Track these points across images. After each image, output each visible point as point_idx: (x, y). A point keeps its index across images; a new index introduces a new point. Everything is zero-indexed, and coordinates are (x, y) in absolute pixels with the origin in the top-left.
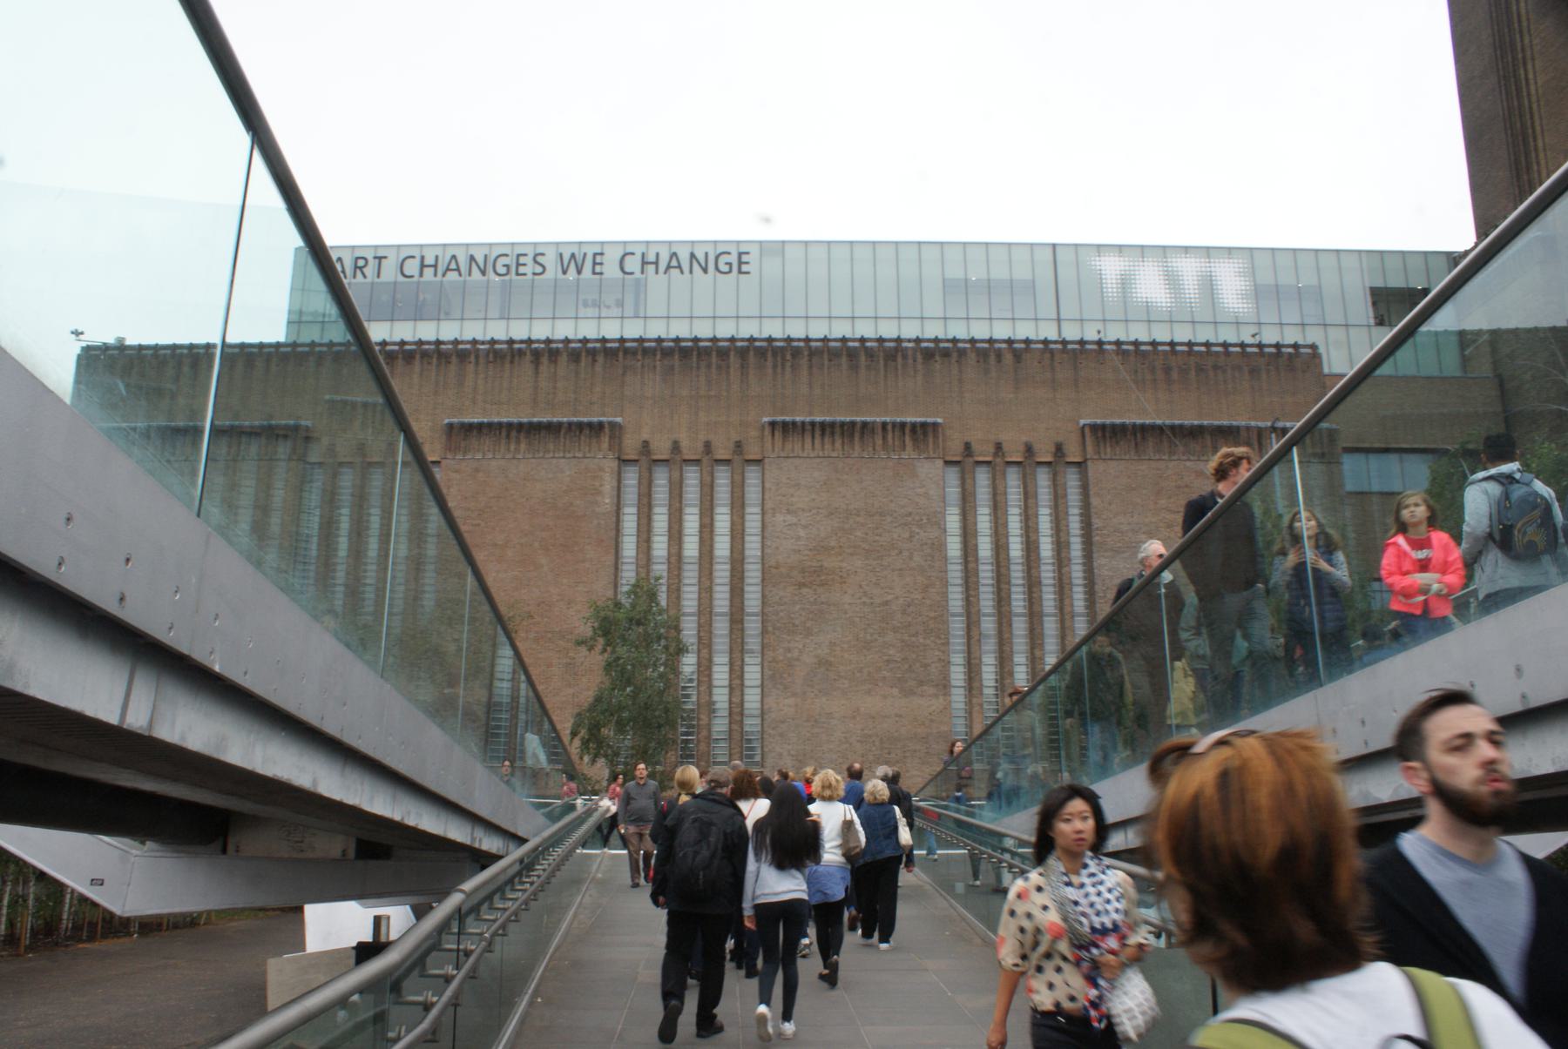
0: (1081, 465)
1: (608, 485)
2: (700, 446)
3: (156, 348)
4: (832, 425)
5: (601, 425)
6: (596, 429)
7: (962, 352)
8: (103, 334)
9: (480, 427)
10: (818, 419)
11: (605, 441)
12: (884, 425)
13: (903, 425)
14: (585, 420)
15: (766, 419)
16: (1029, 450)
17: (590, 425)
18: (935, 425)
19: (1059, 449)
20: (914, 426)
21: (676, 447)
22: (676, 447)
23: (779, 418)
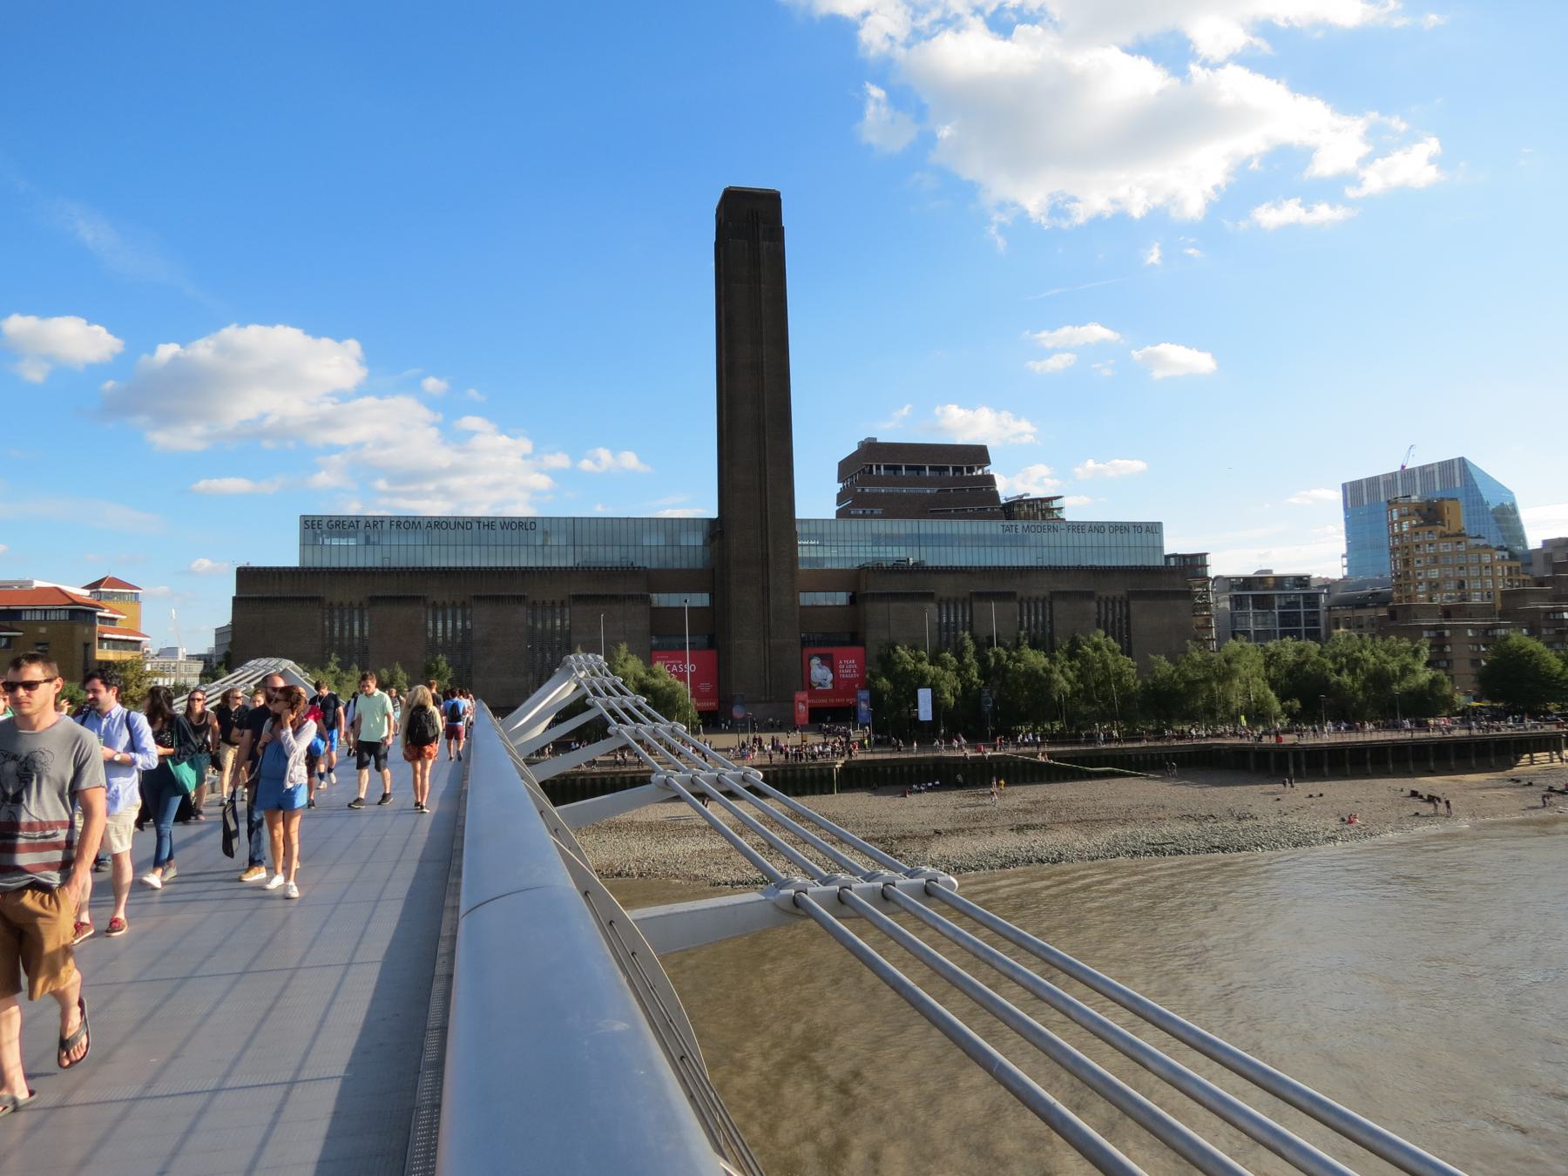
0: (569, 607)
1: (423, 616)
2: (451, 602)
3: (265, 568)
4: (493, 596)
5: (420, 597)
6: (418, 598)
7: (534, 572)
8: (243, 564)
9: (382, 598)
10: (488, 594)
11: (422, 603)
12: (509, 596)
13: (515, 596)
14: (415, 594)
15: (473, 594)
16: (553, 603)
17: (417, 597)
18: (524, 596)
19: (562, 603)
20: (518, 596)
21: (444, 603)
22: (444, 603)
23: (476, 594)
